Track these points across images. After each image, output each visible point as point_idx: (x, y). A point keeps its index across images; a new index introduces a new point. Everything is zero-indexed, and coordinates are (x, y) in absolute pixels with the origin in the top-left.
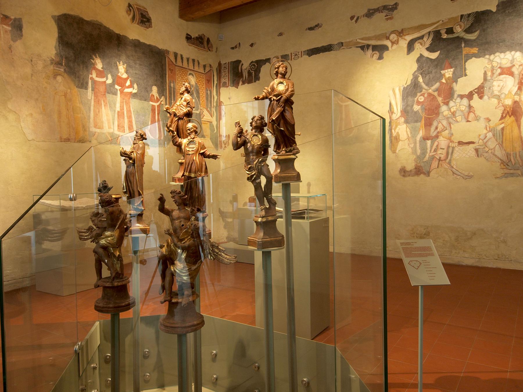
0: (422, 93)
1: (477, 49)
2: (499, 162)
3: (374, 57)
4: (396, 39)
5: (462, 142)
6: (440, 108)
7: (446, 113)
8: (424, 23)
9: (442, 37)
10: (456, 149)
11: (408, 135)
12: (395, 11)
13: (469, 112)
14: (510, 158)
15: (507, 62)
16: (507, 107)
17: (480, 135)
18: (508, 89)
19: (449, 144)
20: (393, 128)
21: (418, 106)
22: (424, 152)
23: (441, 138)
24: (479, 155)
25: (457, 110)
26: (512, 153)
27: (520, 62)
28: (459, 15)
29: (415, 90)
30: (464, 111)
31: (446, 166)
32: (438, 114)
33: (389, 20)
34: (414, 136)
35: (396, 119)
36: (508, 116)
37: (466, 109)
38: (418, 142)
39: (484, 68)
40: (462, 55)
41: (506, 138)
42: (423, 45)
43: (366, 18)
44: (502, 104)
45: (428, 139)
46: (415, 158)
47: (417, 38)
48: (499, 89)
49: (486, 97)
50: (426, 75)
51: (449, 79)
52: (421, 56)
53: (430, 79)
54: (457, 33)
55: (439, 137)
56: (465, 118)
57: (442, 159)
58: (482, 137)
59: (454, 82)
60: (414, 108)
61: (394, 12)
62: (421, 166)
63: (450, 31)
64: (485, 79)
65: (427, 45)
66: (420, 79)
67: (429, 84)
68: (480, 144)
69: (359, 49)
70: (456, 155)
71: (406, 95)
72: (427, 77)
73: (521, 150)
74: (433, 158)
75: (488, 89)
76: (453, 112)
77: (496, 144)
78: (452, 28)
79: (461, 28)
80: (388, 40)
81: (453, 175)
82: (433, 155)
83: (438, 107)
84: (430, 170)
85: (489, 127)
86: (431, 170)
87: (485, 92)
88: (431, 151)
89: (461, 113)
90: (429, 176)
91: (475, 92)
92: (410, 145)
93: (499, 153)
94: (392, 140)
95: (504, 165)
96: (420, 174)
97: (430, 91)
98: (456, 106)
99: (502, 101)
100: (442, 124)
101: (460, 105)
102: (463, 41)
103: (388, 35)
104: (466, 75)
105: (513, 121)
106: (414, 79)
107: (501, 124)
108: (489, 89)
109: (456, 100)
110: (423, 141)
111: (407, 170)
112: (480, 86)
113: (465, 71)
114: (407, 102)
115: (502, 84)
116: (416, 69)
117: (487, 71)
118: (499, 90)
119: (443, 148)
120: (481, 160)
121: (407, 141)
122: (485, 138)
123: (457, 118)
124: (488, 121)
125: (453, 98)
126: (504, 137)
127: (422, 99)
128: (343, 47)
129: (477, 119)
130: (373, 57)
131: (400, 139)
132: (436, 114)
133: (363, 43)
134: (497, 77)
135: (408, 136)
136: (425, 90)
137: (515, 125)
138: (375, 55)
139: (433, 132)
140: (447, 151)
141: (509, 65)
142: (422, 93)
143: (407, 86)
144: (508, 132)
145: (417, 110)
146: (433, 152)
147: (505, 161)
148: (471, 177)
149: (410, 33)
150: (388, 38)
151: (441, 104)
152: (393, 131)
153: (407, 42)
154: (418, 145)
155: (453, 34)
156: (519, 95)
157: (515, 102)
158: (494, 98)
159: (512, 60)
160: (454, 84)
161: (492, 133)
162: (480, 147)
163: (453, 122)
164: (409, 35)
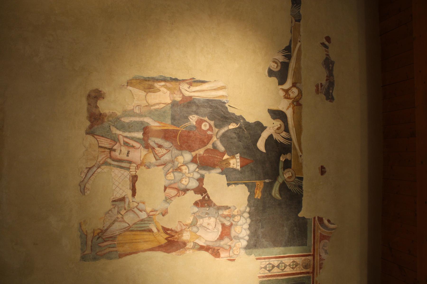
0: (214, 128)
1: (259, 198)
2: (104, 227)
3: (274, 64)
4: (292, 95)
5: (137, 180)
6: (189, 152)
7: (181, 159)
8: (303, 134)
9: (282, 155)
10: (126, 173)
11: (154, 105)
12: (324, 97)
13: (178, 190)
14: (109, 241)
15: (237, 231)
16: (180, 235)
17: (144, 203)
18: (203, 235)
19: (135, 163)
20: (168, 84)
21: (196, 122)
22: (124, 127)
23: (144, 152)
24: (114, 203)
25: (183, 173)
26: (115, 242)
27: (235, 246)
28: (303, 175)
29: (219, 118)
30: (181, 183)
31: (101, 158)
32: (181, 148)
33: (315, 88)
34: (151, 114)
35: (180, 90)
36: (167, 236)
37: (183, 185)
38: (141, 119)
39: (234, 206)
40: (256, 180)
41: (137, 234)
42: (277, 130)
43: (325, 58)
44: (184, 229)
45: (144, 134)
46: (117, 115)
47: (287, 123)
48: (205, 224)
49: (196, 209)
50: (238, 134)
51: (226, 164)
52: (263, 128)
53: (231, 138)
54: (283, 173)
55: (147, 150)
56: (172, 184)
57: (113, 153)
58: (141, 206)
59: (222, 170)
60: (194, 116)
61: (324, 96)
62: (103, 122)
63: (287, 165)
64: (219, 208)
65: (275, 136)
66: (233, 126)
67: (224, 138)
68: (131, 204)
69: (288, 44)
70: (117, 172)
71: (213, 104)
72: (234, 135)
73: (118, 253)
74: (114, 141)
75: (208, 212)
76: (180, 169)
77: (129, 223)
78: (290, 168)
79: (288, 178)
80: (291, 85)
81: (87, 168)
82: (119, 140)
83: (190, 149)
84: (96, 135)
85: (154, 215)
86: (96, 137)
87: (203, 208)
88: (126, 137)
89: (178, 178)
90: (87, 133)
91: (205, 196)
92: (137, 107)
93: (117, 226)
94: (149, 81)
95: (98, 234)
96: (90, 121)
97: (214, 139)
98: (189, 173)
99: (188, 228)
100: (164, 154)
101: (189, 177)
102: (272, 180)
103: (298, 85)
104: (229, 185)
105: (160, 243)
106: (234, 117)
107: (156, 228)
108: (207, 214)
109: (198, 172)
110: (143, 127)
111: (99, 102)
112: (212, 202)
113: (235, 184)
114: (203, 106)
115: (210, 227)
116: (247, 120)
117: (229, 210)
118: (204, 225)
119: (129, 155)
120: (108, 205)
121: (144, 103)
122: (139, 209)
123: (172, 175)
124: (163, 213)
125: (201, 169)
126: (138, 233)
127: (205, 127)
128: (294, 21)
129: (168, 199)
130: (274, 62)
131: (150, 94)
132: (181, 146)
133: (294, 50)
134: (220, 221)
135: (152, 106)
136: (217, 133)
137: (156, 244)
138: (276, 65)
139: (154, 142)
140: (124, 160)
141: (233, 233)
142: (214, 128)
143: (227, 108)
144: (145, 237)
145: (190, 120)
146: (124, 141)
147: (105, 234)
148: (83, 191)
149: (295, 114)
150: (294, 85)
151: (194, 154)
152: (163, 83)
153: (284, 110)
154: (137, 119)
155: (282, 169)
156: (193, 248)
157: (185, 244)
158: (193, 219)
159: (238, 237)
160: (220, 171)
161: (146, 218)
162: (127, 203)
163: (166, 169)
164: (292, 113)
